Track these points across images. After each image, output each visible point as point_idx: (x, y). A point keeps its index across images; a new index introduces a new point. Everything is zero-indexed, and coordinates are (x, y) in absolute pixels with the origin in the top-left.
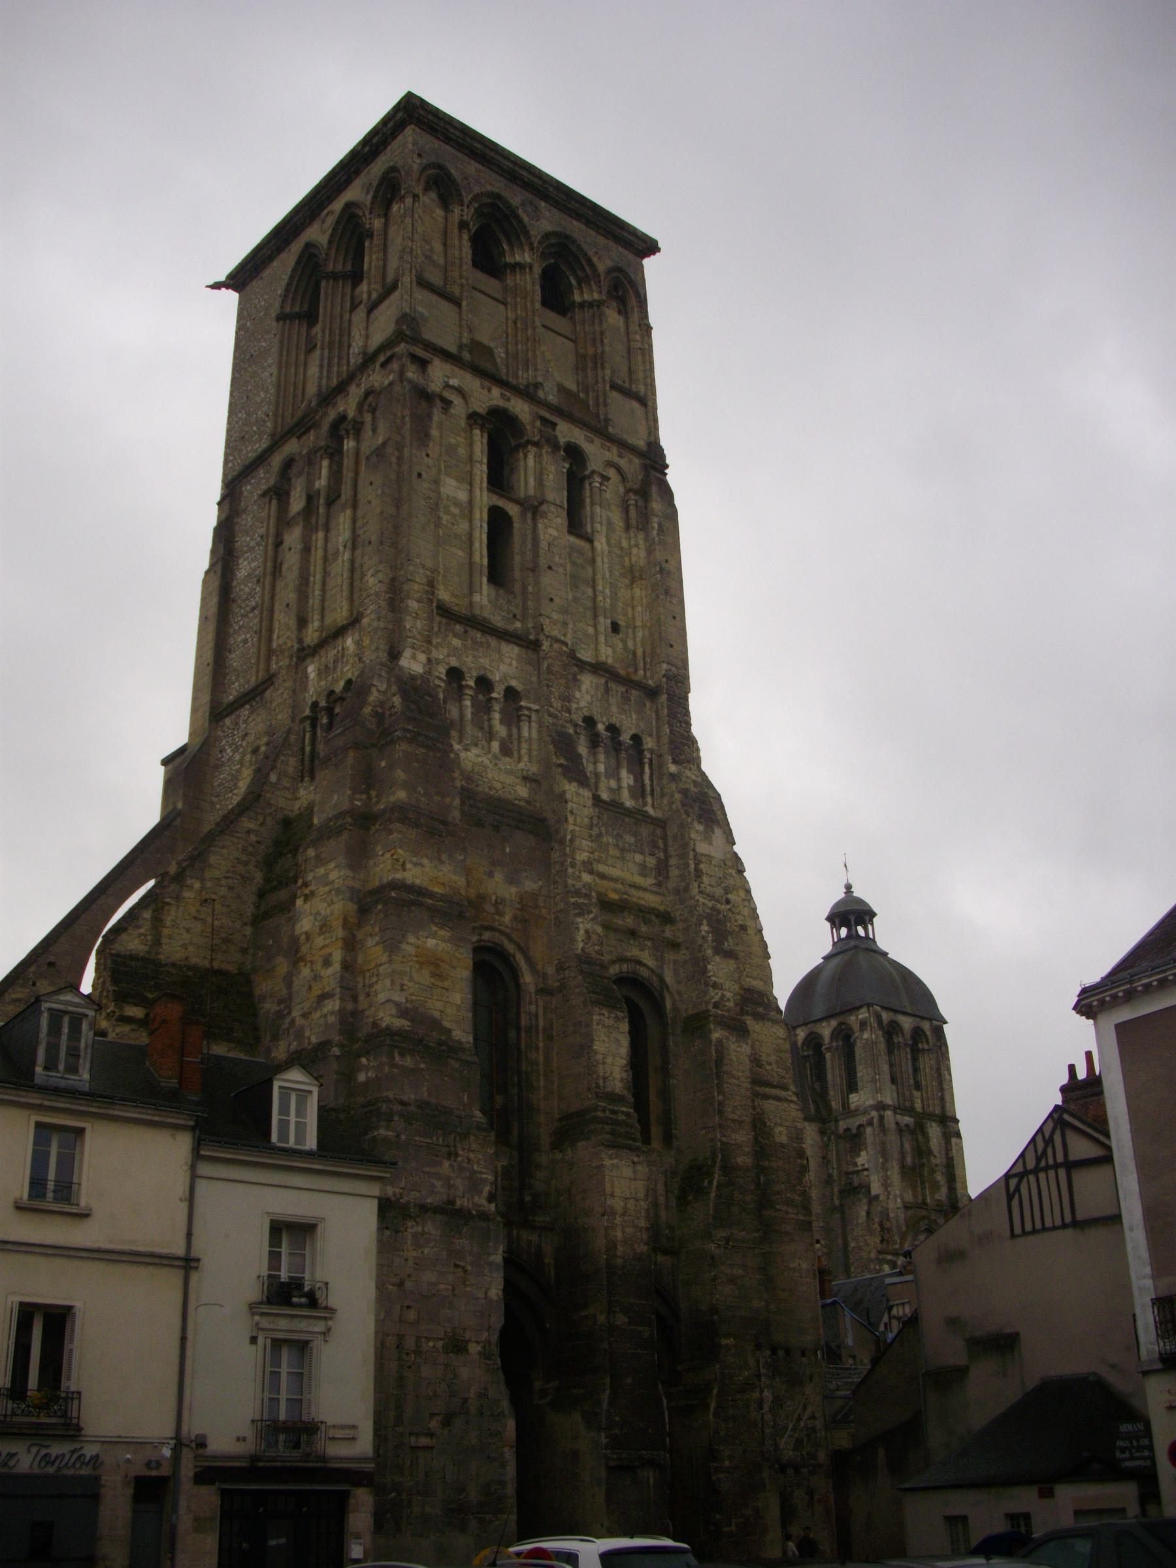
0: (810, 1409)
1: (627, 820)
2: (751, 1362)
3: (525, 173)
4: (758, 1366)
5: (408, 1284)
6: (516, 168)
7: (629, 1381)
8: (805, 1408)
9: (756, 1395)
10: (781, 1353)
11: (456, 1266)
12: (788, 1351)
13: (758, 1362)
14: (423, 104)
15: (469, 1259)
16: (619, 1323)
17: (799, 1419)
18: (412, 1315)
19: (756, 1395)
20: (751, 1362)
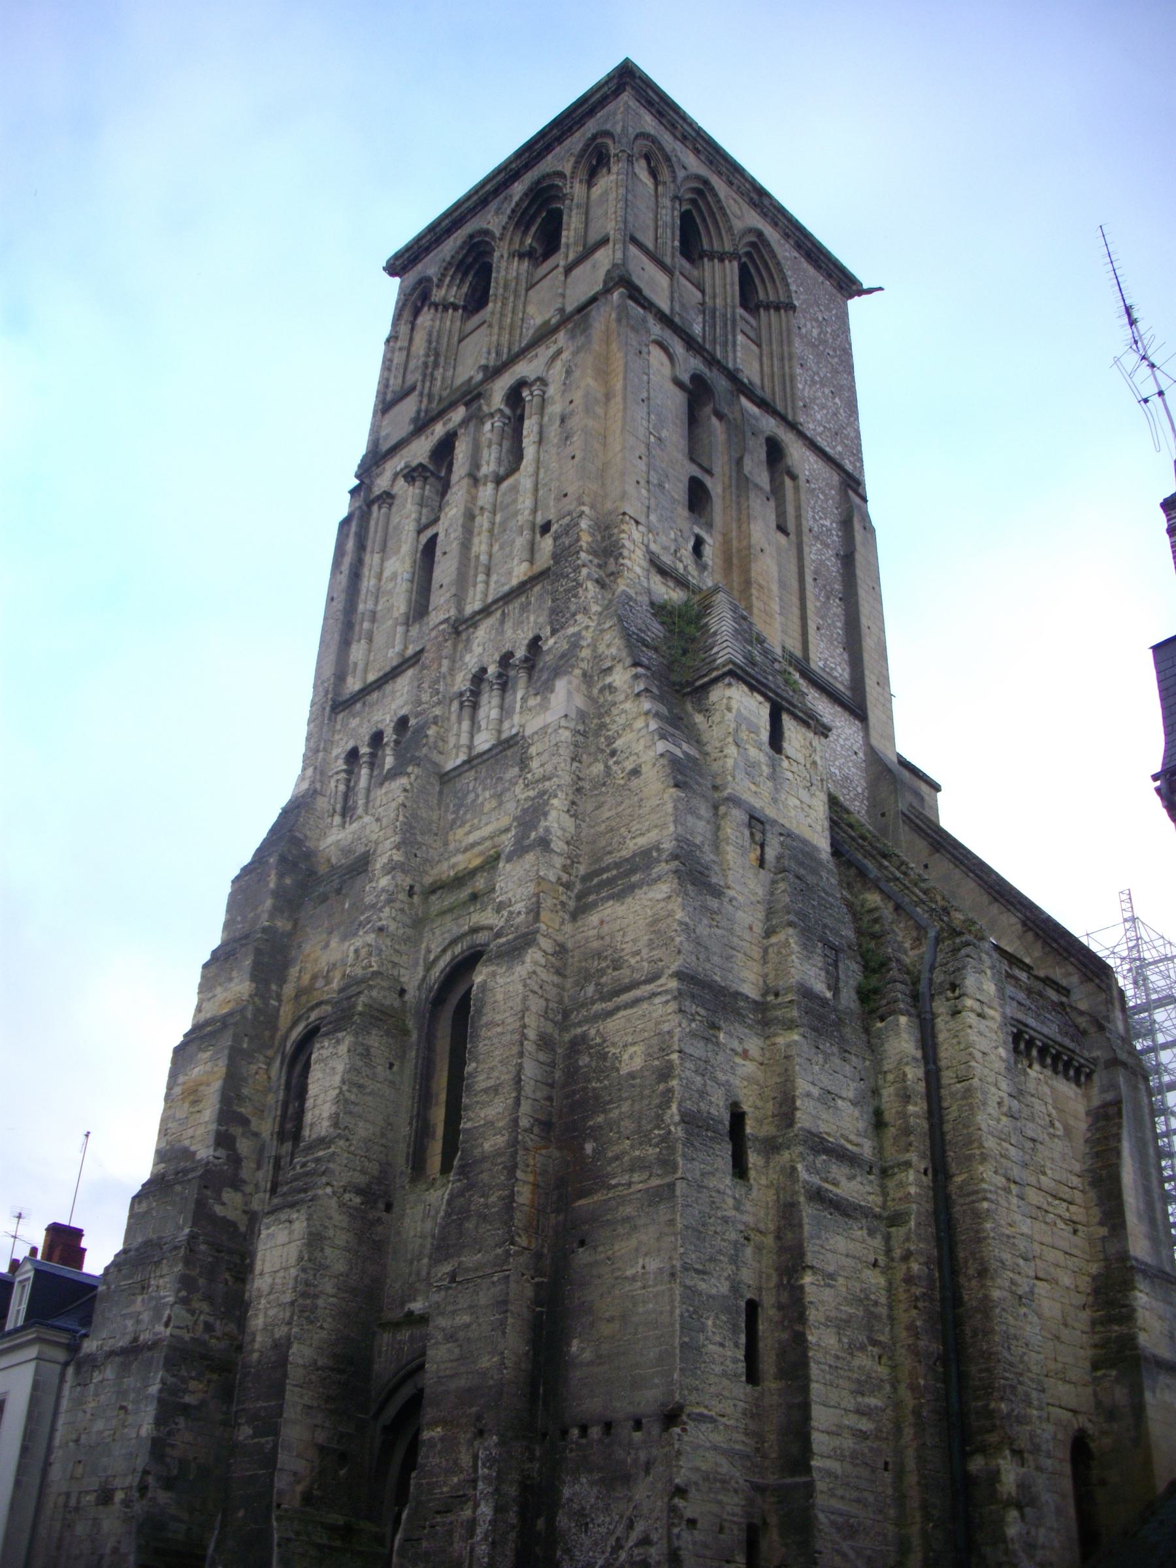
0: (640, 1528)
1: (509, 753)
2: (465, 1459)
3: (488, 187)
4: (475, 1467)
5: (83, 1437)
6: (480, 193)
7: (241, 1514)
8: (631, 1526)
9: (467, 1513)
10: (595, 1432)
11: (122, 1408)
12: (608, 1426)
13: (476, 1457)
14: (397, 256)
15: (132, 1396)
16: (241, 1438)
17: (618, 1546)
18: (80, 1470)
19: (467, 1513)
20: (465, 1459)
